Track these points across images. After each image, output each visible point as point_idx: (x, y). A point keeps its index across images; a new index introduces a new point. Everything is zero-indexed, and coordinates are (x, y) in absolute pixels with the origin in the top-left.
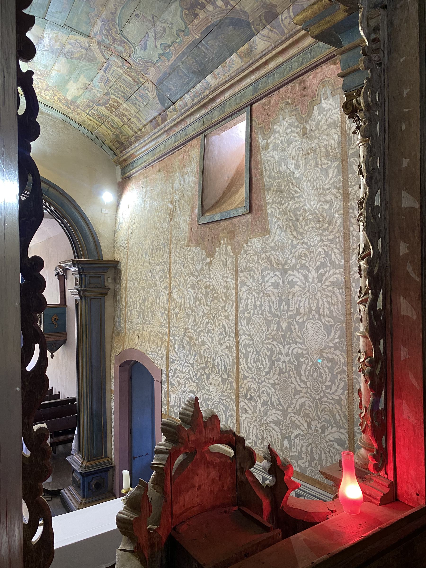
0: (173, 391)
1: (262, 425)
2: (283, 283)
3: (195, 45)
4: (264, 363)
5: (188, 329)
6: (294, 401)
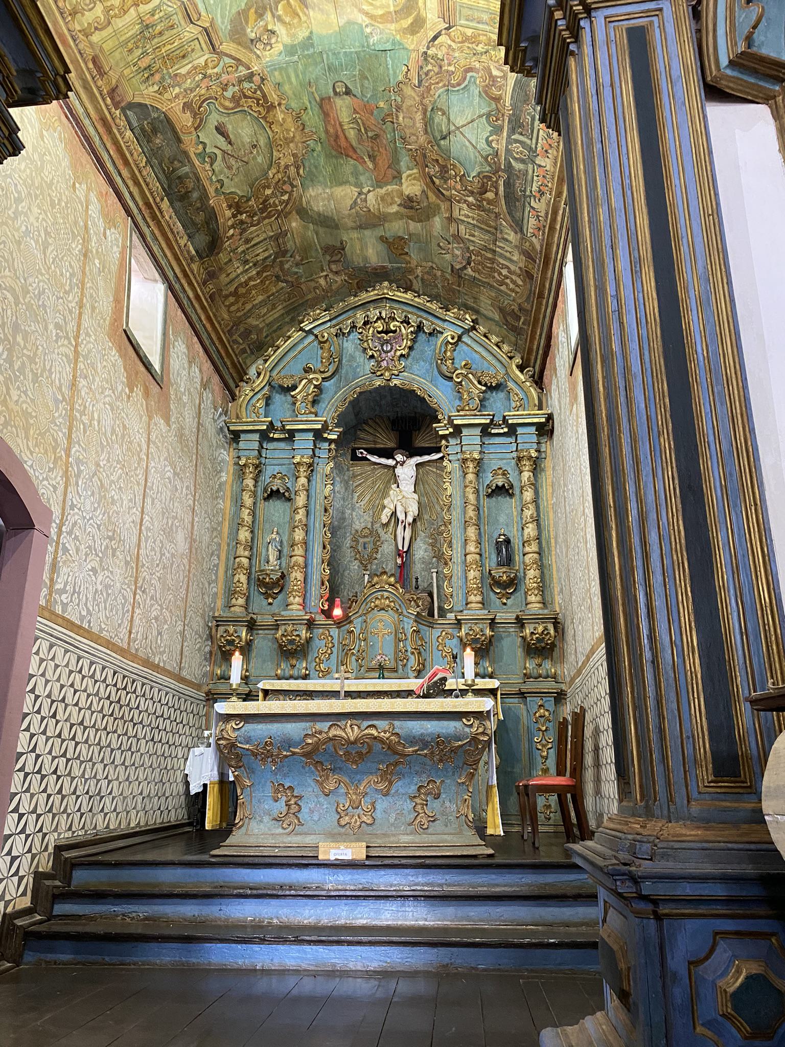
0: (64, 562)
3: (204, 196)
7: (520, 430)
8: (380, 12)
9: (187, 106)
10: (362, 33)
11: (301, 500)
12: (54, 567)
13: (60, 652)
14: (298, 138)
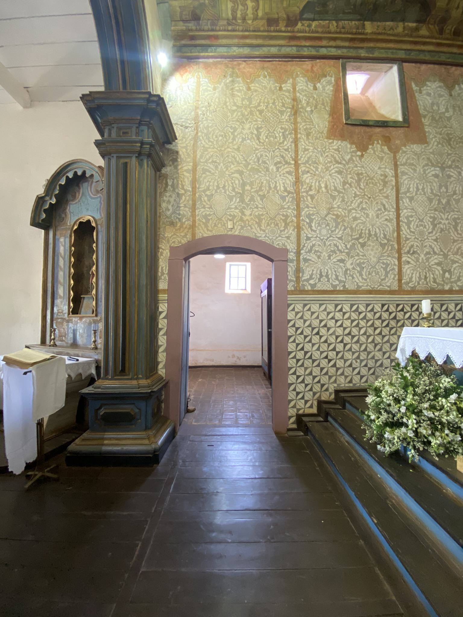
1: (425, 269)
2: (442, 175)
4: (427, 227)
5: (332, 208)
6: (453, 247)
12: (298, 270)
13: (315, 307)
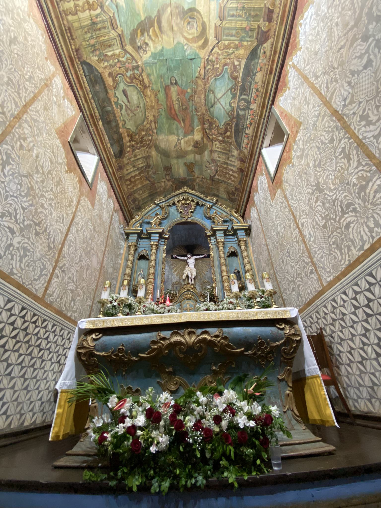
7: (238, 232)
8: (191, 37)
9: (110, 74)
10: (183, 48)
11: (153, 258)
14: (156, 107)
